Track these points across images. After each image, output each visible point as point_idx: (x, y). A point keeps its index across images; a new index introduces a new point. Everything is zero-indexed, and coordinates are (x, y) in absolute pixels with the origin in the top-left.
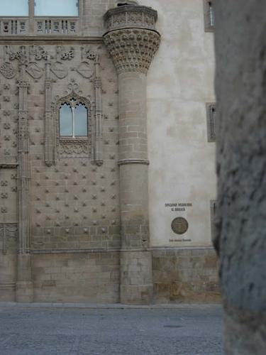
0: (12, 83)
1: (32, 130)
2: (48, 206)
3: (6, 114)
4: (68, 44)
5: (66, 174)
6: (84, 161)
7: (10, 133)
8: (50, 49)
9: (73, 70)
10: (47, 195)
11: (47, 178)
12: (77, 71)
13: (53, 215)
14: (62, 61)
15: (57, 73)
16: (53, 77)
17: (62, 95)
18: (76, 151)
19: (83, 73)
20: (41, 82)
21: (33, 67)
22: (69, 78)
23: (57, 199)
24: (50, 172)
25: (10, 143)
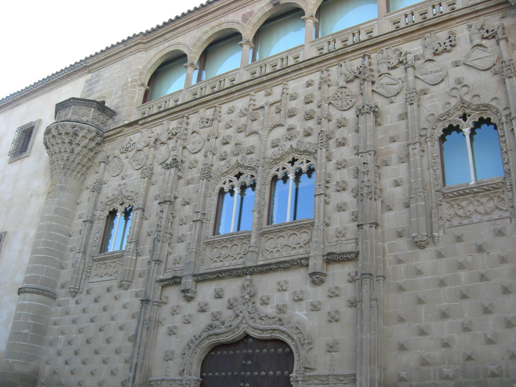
0: (350, 115)
1: (387, 182)
2: (422, 333)
3: (341, 166)
4: (442, 30)
5: (461, 260)
6: (500, 224)
7: (347, 197)
8: (414, 47)
9: (456, 64)
10: (422, 309)
11: (419, 272)
12: (465, 64)
13: (438, 353)
14: (436, 58)
15: (428, 78)
16: (420, 85)
17: (441, 112)
18: (481, 209)
19: (477, 63)
20: (400, 100)
21: (385, 80)
22: (450, 82)
23: (444, 315)
24: (426, 259)
25: (346, 216)
